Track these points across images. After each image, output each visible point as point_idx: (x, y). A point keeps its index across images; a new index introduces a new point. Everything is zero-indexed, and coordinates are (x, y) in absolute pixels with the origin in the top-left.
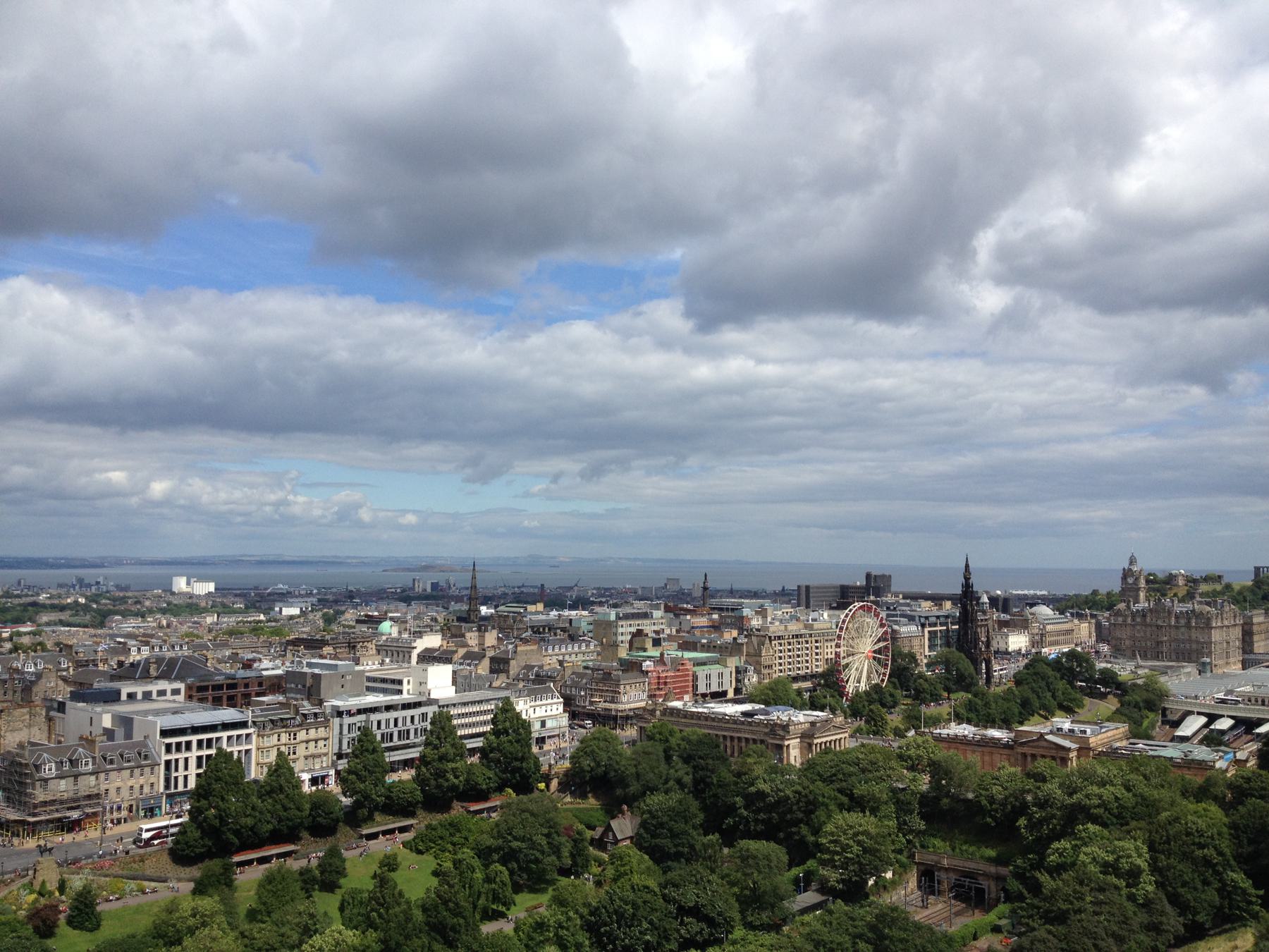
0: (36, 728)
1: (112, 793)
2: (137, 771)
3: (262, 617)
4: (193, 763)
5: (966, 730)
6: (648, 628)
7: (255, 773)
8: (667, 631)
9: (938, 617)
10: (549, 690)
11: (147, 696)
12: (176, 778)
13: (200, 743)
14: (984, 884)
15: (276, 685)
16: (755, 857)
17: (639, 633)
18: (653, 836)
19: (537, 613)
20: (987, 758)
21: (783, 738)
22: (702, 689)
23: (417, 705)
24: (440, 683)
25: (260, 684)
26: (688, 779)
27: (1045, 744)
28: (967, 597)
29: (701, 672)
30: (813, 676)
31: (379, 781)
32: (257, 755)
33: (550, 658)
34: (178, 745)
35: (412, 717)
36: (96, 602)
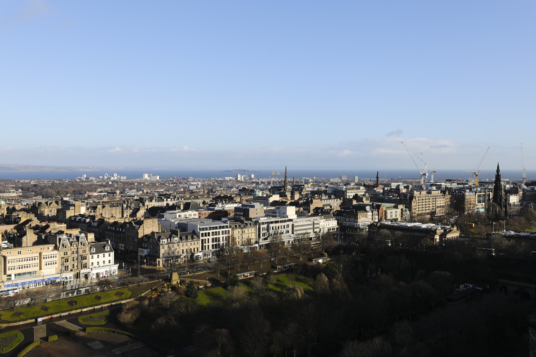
2: (193, 242)
4: (211, 241)
17: (356, 195)
34: (206, 233)
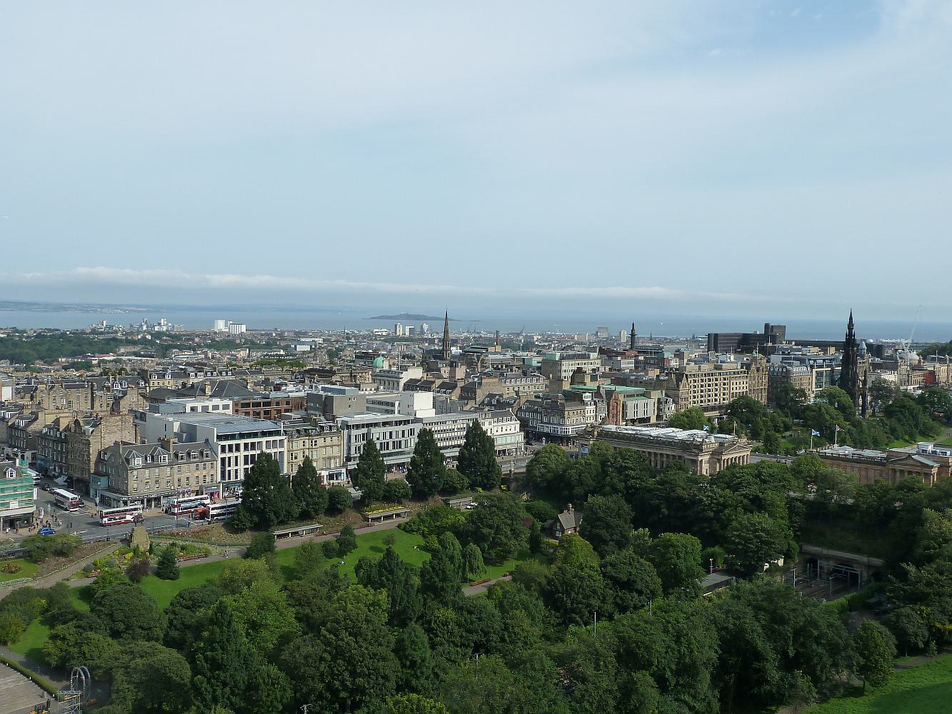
0: (126, 432)
1: (184, 481)
2: (201, 465)
3: (282, 352)
5: (848, 450)
6: (588, 368)
7: (289, 470)
8: (602, 369)
9: (824, 360)
10: (508, 414)
11: (205, 409)
12: (229, 471)
13: (246, 445)
14: (858, 570)
15: (298, 404)
16: (672, 546)
17: (579, 370)
18: (592, 527)
19: (496, 353)
20: (863, 473)
21: (697, 455)
22: (630, 416)
23: (406, 422)
24: (423, 404)
25: (288, 403)
26: (621, 486)
27: (911, 462)
28: (849, 345)
29: (630, 404)
30: (720, 407)
31: (379, 480)
32: (289, 454)
33: (507, 389)
34: (230, 446)
35: (403, 432)
36: (160, 339)
